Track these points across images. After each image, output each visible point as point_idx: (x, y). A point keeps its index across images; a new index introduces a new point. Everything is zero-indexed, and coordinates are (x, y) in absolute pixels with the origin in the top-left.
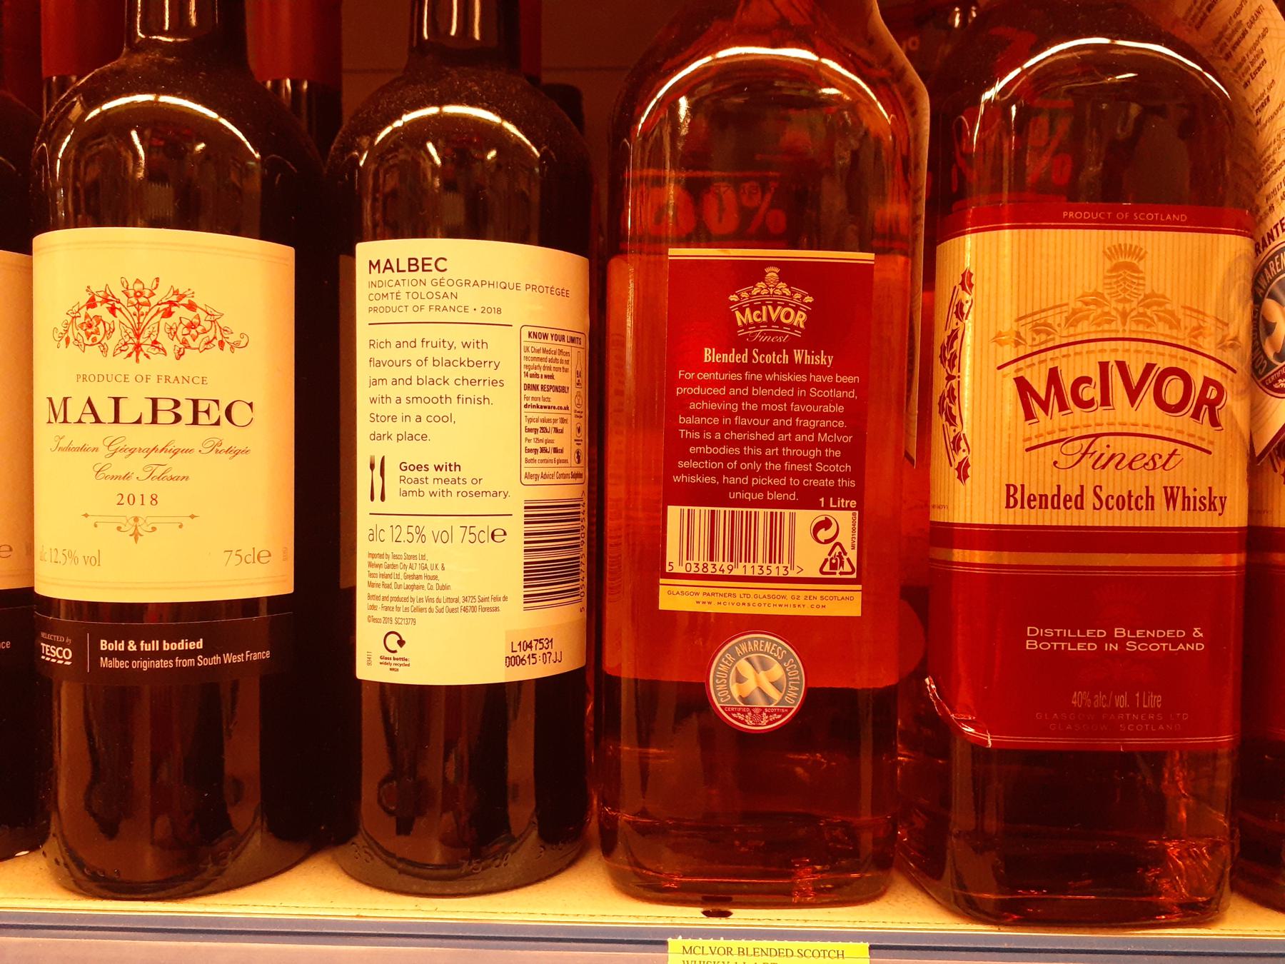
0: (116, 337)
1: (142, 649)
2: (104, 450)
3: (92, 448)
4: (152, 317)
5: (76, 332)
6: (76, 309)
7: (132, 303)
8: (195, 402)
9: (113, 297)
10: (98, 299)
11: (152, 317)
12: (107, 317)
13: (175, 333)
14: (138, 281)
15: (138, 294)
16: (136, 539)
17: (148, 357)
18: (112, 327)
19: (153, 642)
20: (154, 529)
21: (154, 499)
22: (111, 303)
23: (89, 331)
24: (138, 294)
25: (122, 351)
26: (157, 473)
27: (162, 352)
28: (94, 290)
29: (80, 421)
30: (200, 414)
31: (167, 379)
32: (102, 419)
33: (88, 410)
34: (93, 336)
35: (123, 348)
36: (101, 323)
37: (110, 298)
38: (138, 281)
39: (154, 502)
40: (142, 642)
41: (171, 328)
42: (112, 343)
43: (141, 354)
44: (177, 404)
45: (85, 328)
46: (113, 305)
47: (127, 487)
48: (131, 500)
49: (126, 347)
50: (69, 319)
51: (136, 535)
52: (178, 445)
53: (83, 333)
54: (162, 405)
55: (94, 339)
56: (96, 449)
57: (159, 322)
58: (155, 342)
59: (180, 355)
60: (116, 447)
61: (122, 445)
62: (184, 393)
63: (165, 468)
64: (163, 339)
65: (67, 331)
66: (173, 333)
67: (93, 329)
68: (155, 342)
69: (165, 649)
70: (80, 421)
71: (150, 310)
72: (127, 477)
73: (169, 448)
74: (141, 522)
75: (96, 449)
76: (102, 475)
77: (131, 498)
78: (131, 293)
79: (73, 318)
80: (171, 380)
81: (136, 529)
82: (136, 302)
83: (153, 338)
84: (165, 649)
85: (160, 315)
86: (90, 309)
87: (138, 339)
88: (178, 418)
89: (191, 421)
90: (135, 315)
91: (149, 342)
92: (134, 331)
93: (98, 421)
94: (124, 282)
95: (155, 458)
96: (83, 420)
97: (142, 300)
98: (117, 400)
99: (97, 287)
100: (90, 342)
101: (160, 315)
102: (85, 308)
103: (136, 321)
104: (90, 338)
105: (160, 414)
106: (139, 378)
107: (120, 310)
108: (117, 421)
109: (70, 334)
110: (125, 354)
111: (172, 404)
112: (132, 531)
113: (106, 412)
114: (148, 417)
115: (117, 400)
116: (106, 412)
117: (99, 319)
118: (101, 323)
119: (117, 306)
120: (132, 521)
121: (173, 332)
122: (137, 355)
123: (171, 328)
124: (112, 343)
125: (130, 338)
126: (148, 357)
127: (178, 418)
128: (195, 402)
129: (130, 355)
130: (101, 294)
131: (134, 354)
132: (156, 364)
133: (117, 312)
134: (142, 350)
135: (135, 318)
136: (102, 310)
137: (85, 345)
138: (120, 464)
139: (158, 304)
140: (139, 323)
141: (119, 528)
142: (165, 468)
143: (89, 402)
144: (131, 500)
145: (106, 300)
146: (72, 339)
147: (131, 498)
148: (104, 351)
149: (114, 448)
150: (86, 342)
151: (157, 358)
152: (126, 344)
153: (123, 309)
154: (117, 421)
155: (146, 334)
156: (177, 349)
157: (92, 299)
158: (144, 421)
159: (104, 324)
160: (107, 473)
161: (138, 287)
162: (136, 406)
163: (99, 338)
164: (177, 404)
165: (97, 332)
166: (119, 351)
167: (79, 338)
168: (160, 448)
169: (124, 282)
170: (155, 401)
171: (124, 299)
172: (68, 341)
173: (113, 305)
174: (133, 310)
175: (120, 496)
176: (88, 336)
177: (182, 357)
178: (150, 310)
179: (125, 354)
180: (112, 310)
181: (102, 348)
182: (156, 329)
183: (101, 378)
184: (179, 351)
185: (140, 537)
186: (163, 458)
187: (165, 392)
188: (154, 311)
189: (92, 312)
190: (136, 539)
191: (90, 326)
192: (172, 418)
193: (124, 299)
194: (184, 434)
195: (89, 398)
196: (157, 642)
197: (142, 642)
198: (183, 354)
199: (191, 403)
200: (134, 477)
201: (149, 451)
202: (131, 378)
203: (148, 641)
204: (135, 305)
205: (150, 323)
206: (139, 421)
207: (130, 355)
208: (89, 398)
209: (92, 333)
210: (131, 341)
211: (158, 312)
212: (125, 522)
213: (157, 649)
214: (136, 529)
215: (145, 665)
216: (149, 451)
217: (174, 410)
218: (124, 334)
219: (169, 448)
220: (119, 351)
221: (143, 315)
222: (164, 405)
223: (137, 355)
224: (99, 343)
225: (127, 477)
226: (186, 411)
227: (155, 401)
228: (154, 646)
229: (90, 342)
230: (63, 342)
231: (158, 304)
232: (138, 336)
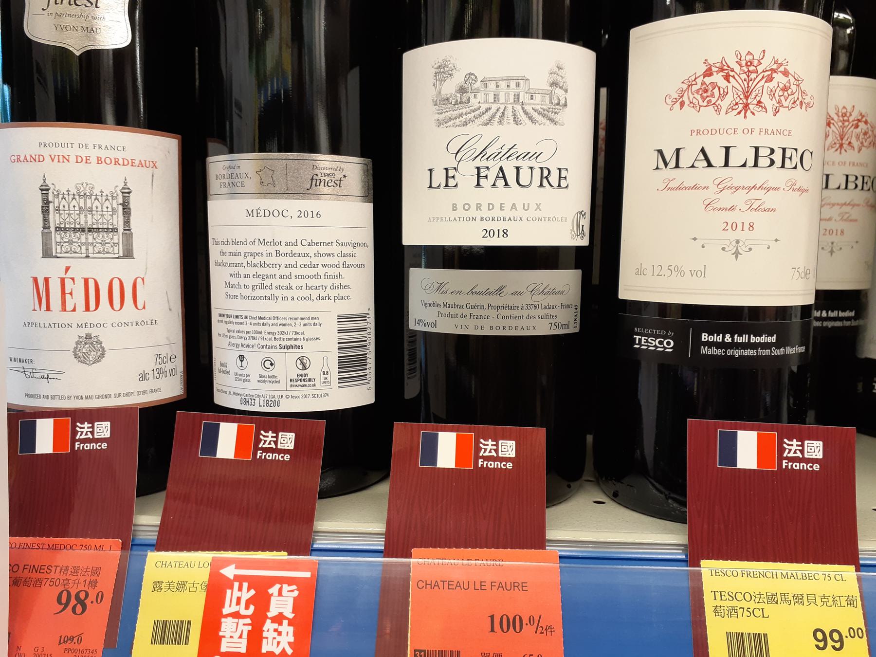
0: (729, 99)
1: (736, 341)
2: (713, 188)
3: (703, 186)
4: (758, 82)
5: (691, 97)
6: (693, 78)
7: (744, 71)
8: (784, 150)
9: (728, 67)
10: (714, 69)
11: (758, 82)
12: (722, 83)
13: (774, 94)
14: (749, 53)
15: (749, 64)
16: (737, 257)
17: (753, 114)
18: (726, 90)
19: (744, 336)
20: (750, 249)
21: (751, 226)
22: (726, 71)
23: (705, 95)
24: (749, 64)
25: (733, 109)
26: (755, 206)
27: (764, 110)
28: (711, 62)
29: (693, 166)
30: (786, 159)
31: (766, 132)
32: (713, 162)
33: (701, 157)
34: (708, 99)
35: (734, 108)
36: (717, 88)
37: (726, 68)
38: (749, 53)
39: (751, 229)
40: (736, 335)
41: (771, 91)
42: (725, 104)
43: (749, 112)
44: (772, 151)
45: (700, 93)
46: (728, 73)
47: (730, 217)
48: (734, 226)
49: (737, 107)
50: (685, 87)
51: (737, 254)
52: (770, 184)
53: (698, 97)
54: (762, 152)
55: (710, 101)
56: (706, 188)
57: (763, 86)
58: (759, 102)
59: (776, 112)
60: (725, 185)
61: (729, 184)
62: (777, 143)
63: (760, 202)
64: (766, 99)
65: (682, 96)
66: (772, 94)
67: (709, 93)
68: (759, 102)
69: (752, 341)
70: (693, 166)
71: (757, 76)
72: (732, 209)
73: (764, 186)
74: (741, 243)
75: (706, 188)
76: (711, 208)
77: (734, 225)
78: (744, 63)
79: (689, 86)
80: (769, 132)
81: (737, 249)
82: (746, 70)
83: (758, 99)
84: (752, 341)
85: (764, 80)
86: (706, 78)
87: (747, 100)
88: (772, 162)
89: (780, 166)
90: (745, 80)
91: (755, 102)
92: (744, 93)
93: (710, 165)
94: (738, 55)
95: (754, 194)
96: (695, 165)
97: (751, 68)
98: (727, 149)
99: (715, 59)
100: (705, 103)
101: (764, 80)
102: (702, 77)
103: (746, 86)
104: (706, 101)
105: (760, 159)
106: (746, 131)
107: (733, 77)
108: (726, 164)
109: (685, 98)
110: (736, 112)
111: (769, 151)
112: (733, 251)
113: (718, 158)
114: (751, 162)
115: (727, 149)
116: (718, 158)
117: (714, 85)
118: (717, 88)
119: (732, 74)
120: (734, 243)
121: (772, 94)
122: (745, 113)
123: (771, 91)
124: (725, 104)
125: (740, 99)
126: (753, 114)
127: (772, 162)
128: (784, 150)
129: (739, 113)
130: (718, 65)
131: (743, 112)
132: (759, 120)
133: (731, 79)
134: (749, 108)
135: (745, 83)
136: (718, 78)
137: (701, 106)
138: (727, 199)
139: (763, 72)
140: (748, 87)
141: (723, 249)
142: (760, 202)
143: (703, 151)
144: (734, 226)
145: (722, 70)
146: (687, 102)
147: (734, 225)
148: (718, 110)
149: (722, 186)
150: (701, 103)
151: (760, 115)
152: (737, 104)
153: (736, 76)
154: (726, 164)
155: (753, 96)
156: (775, 107)
157: (710, 69)
158: (748, 164)
159: (719, 89)
160: (715, 206)
161: (749, 58)
162: (742, 153)
163: (714, 100)
164: (772, 151)
165: (713, 95)
166: (730, 110)
167: (695, 101)
168: (758, 186)
169: (738, 55)
170: (757, 149)
171: (737, 68)
172: (682, 104)
173: (728, 73)
174: (744, 76)
175: (726, 224)
176: (704, 100)
177: (778, 114)
178: (757, 76)
179: (736, 112)
180: (727, 78)
181: (716, 108)
182: (761, 91)
183: (714, 132)
184: (776, 109)
185: (739, 255)
186: (758, 194)
187: (765, 142)
188: (760, 77)
189: (708, 80)
190: (737, 257)
191: (706, 91)
192: (768, 162)
193: (737, 68)
194: (776, 176)
195: (703, 148)
196: (747, 335)
197: (736, 335)
198: (778, 111)
199: (781, 151)
200: (737, 209)
201: (750, 189)
202: (740, 131)
203: (740, 335)
204: (745, 73)
205: (757, 87)
206: (744, 165)
207: (739, 113)
208: (703, 148)
209: (707, 96)
210: (741, 102)
211: (763, 77)
212: (728, 244)
213: (747, 341)
214: (737, 249)
215: (737, 353)
216: (750, 189)
217: (770, 156)
218: (736, 96)
219: (764, 186)
220: (730, 110)
221: (751, 80)
222: (763, 152)
223: (745, 113)
224: (714, 104)
225: (732, 209)
226: (778, 157)
227: (757, 149)
228: (744, 339)
229: (705, 103)
230: (678, 105)
231: (763, 72)
232: (747, 98)
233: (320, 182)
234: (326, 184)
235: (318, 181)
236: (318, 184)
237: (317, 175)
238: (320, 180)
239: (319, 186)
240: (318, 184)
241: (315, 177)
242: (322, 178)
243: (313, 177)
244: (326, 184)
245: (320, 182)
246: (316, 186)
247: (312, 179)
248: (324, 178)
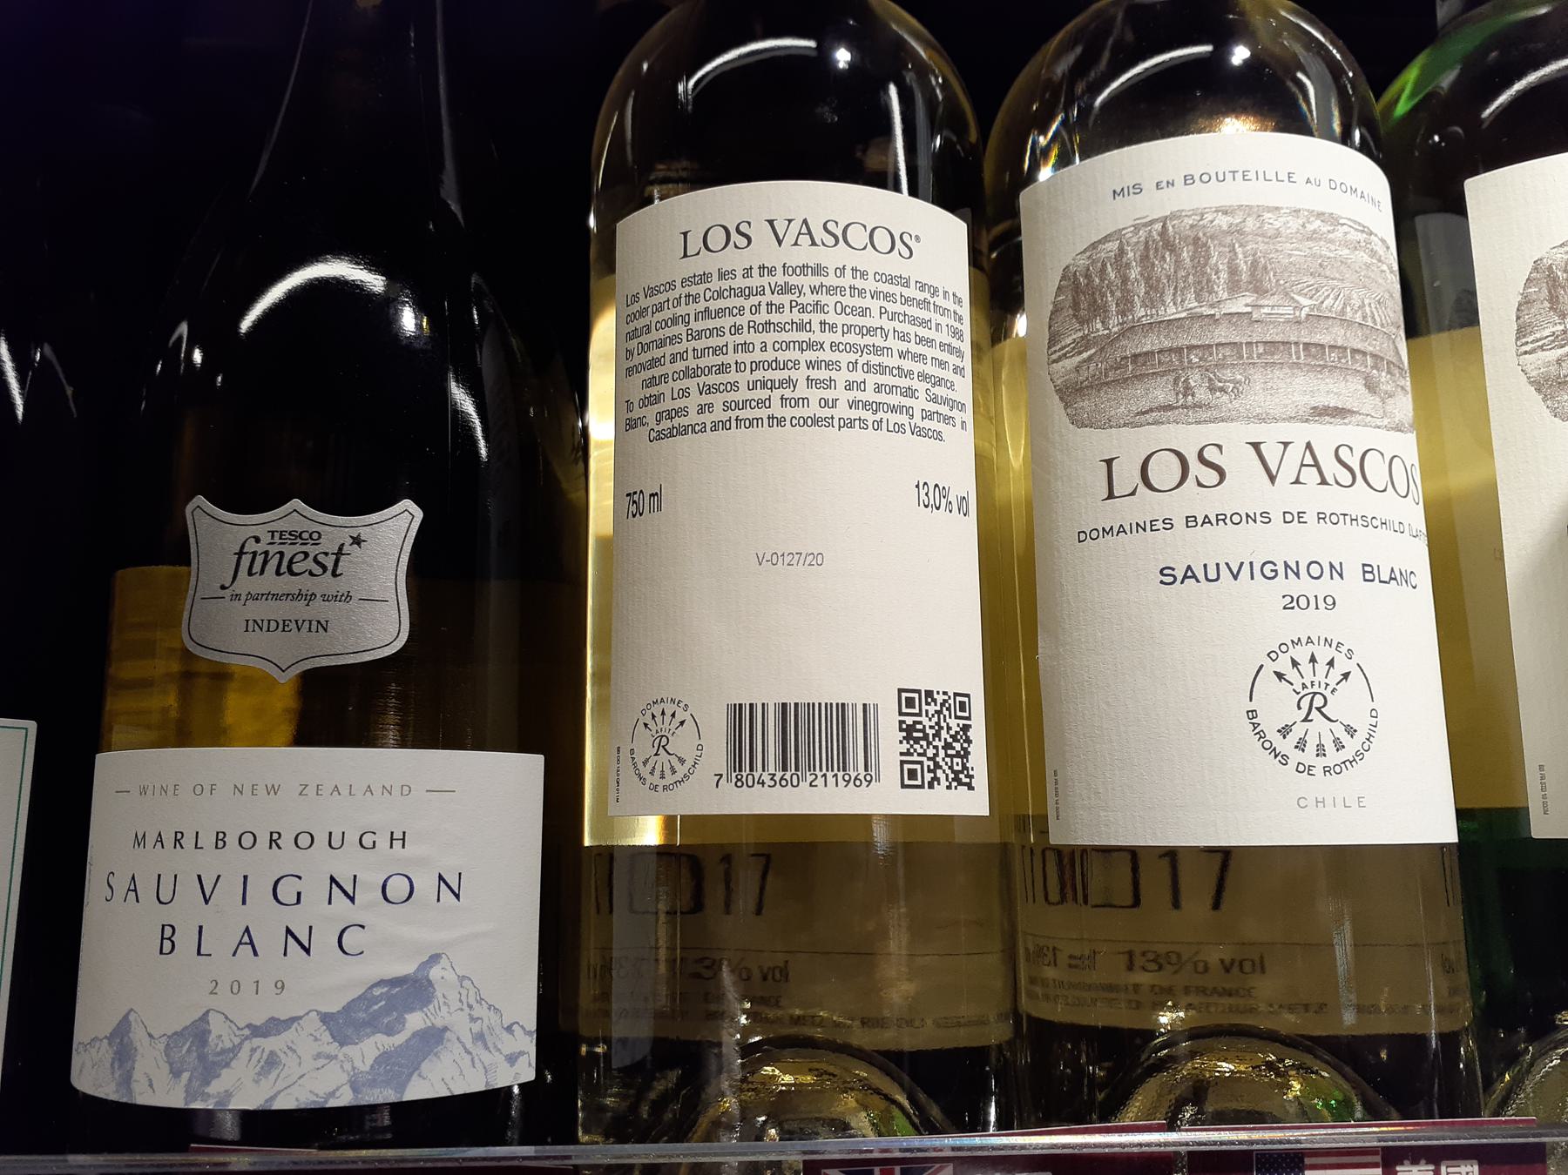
233: (265, 562)
234: (284, 568)
235: (260, 560)
236: (257, 567)
237: (257, 540)
238: (266, 553)
239: (262, 572)
240: (257, 567)
241: (251, 546)
242: (273, 550)
243: (243, 546)
244: (284, 568)
245: (265, 562)
246: (250, 574)
247: (241, 553)
248: (281, 548)
